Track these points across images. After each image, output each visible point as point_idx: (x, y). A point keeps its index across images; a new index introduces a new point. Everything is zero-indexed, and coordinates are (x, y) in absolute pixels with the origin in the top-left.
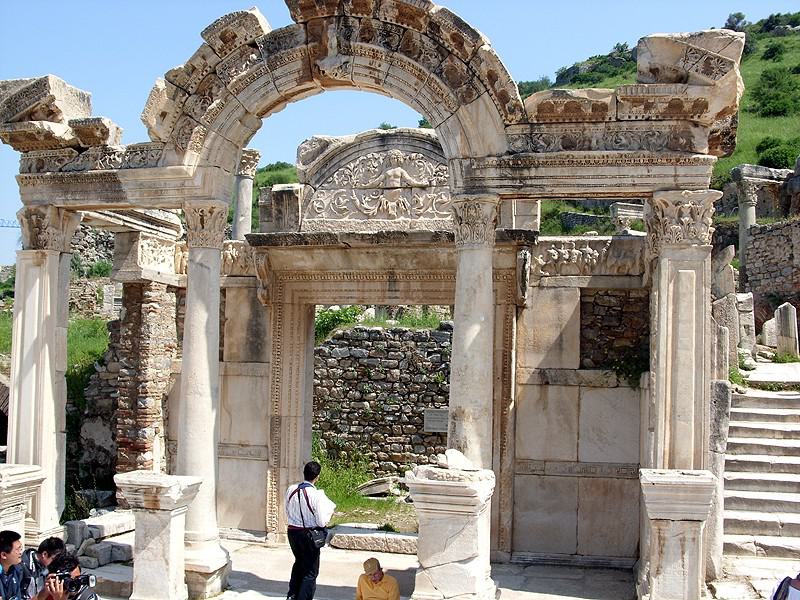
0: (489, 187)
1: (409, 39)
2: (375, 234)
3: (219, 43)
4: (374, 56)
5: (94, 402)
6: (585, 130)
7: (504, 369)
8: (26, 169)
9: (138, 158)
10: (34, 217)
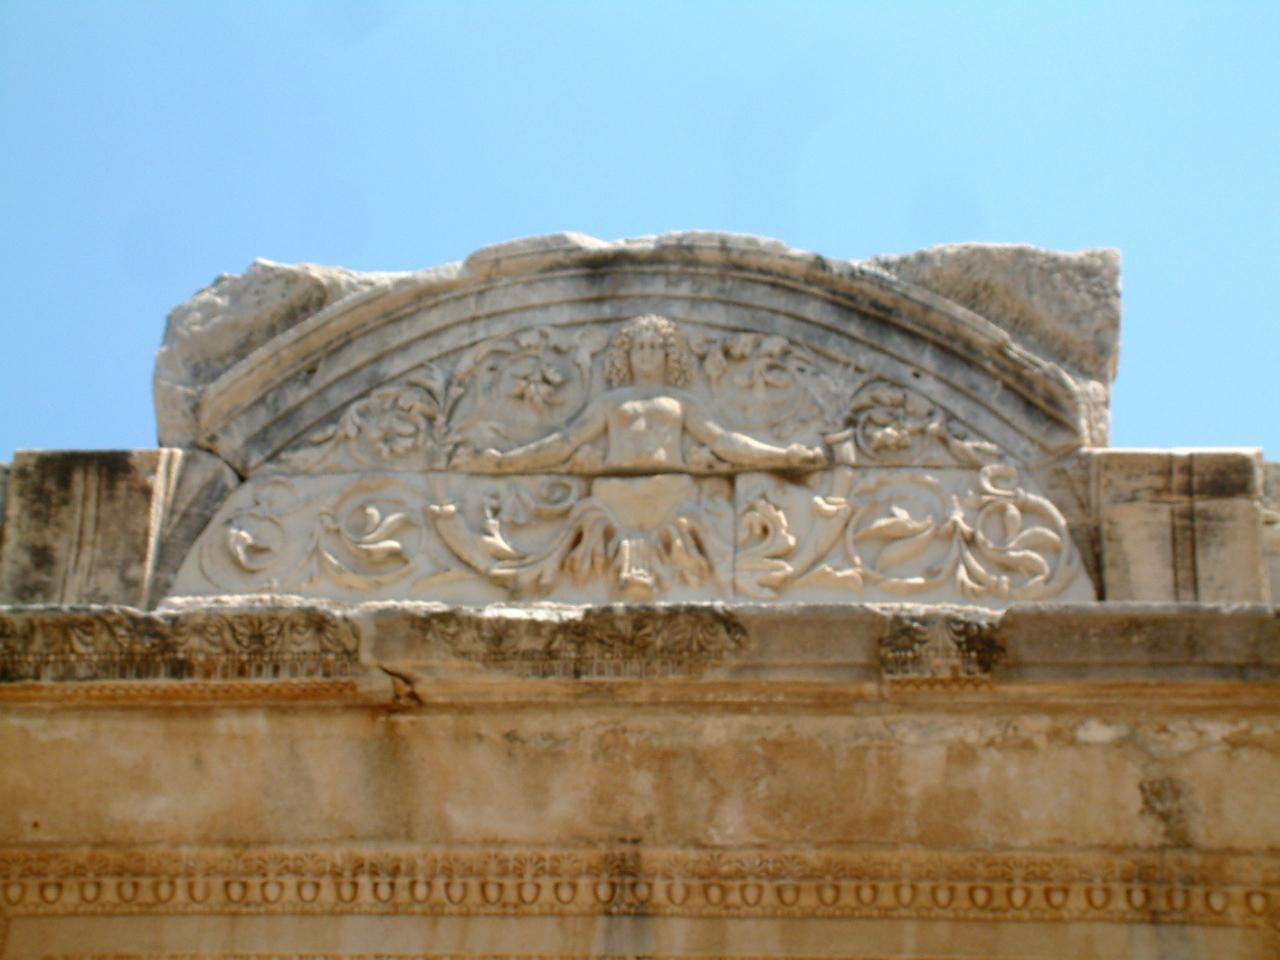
2: (565, 628)
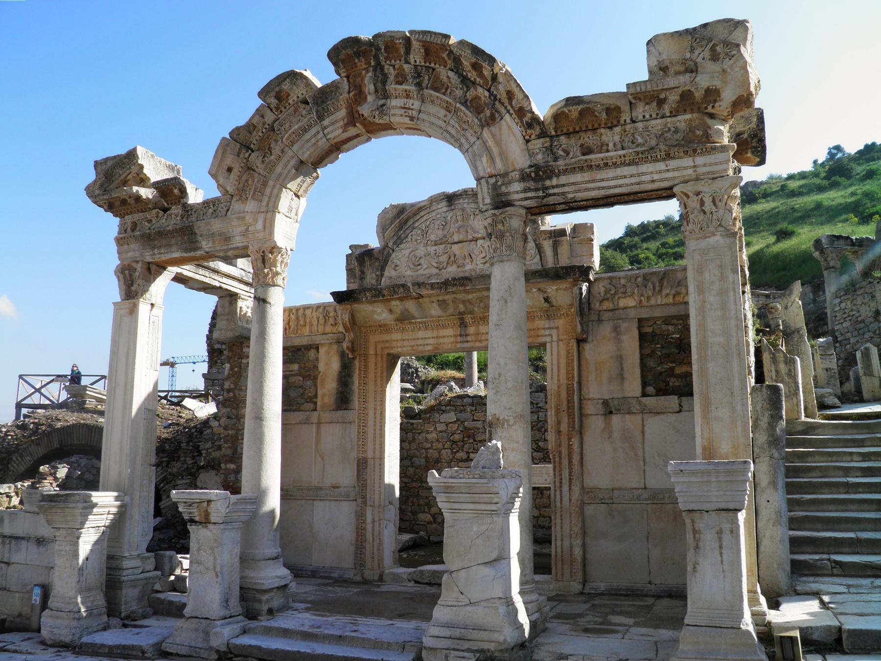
0: (515, 200)
1: (437, 78)
2: (442, 283)
3: (273, 101)
4: (408, 96)
5: (209, 454)
6: (601, 135)
7: (568, 401)
8: (123, 230)
9: (211, 210)
10: (127, 272)
